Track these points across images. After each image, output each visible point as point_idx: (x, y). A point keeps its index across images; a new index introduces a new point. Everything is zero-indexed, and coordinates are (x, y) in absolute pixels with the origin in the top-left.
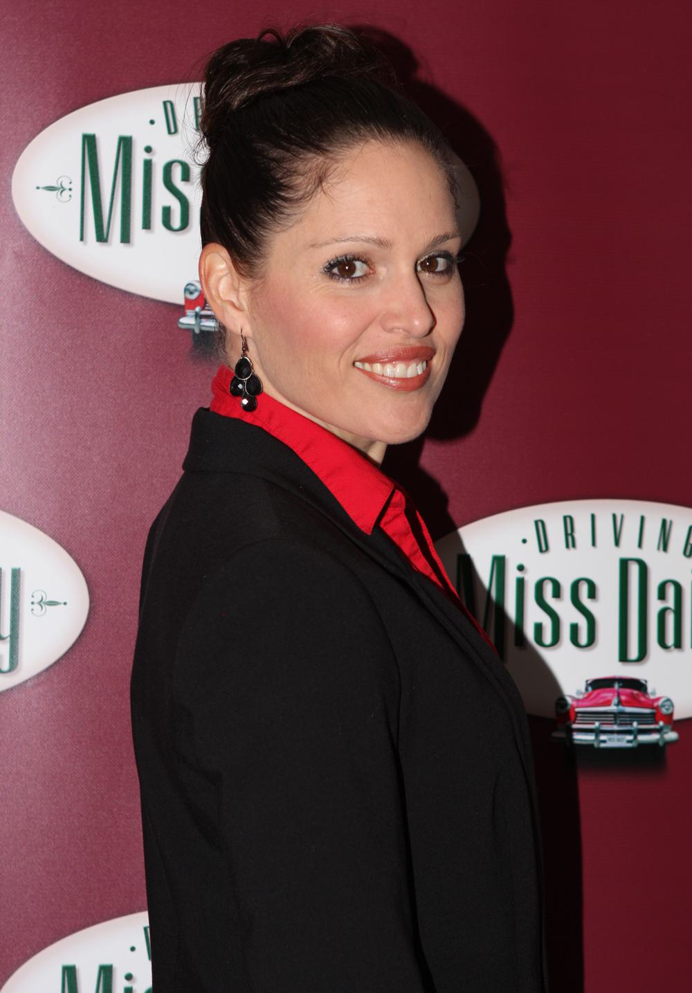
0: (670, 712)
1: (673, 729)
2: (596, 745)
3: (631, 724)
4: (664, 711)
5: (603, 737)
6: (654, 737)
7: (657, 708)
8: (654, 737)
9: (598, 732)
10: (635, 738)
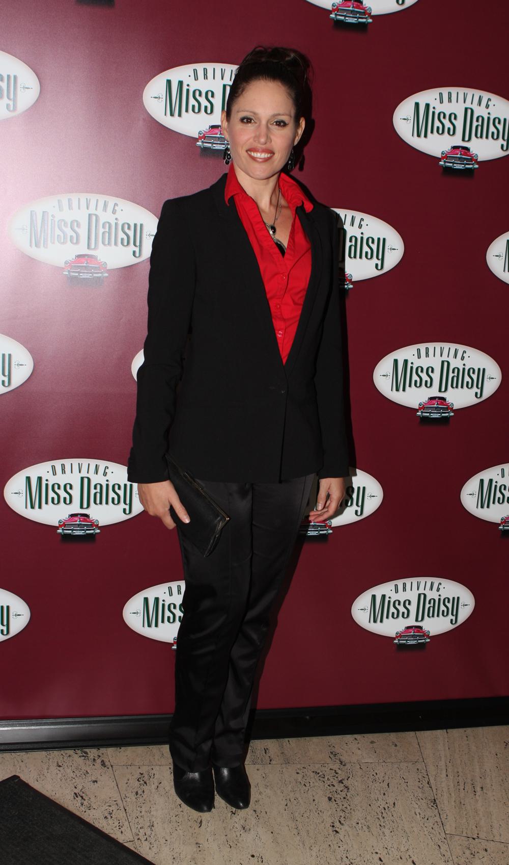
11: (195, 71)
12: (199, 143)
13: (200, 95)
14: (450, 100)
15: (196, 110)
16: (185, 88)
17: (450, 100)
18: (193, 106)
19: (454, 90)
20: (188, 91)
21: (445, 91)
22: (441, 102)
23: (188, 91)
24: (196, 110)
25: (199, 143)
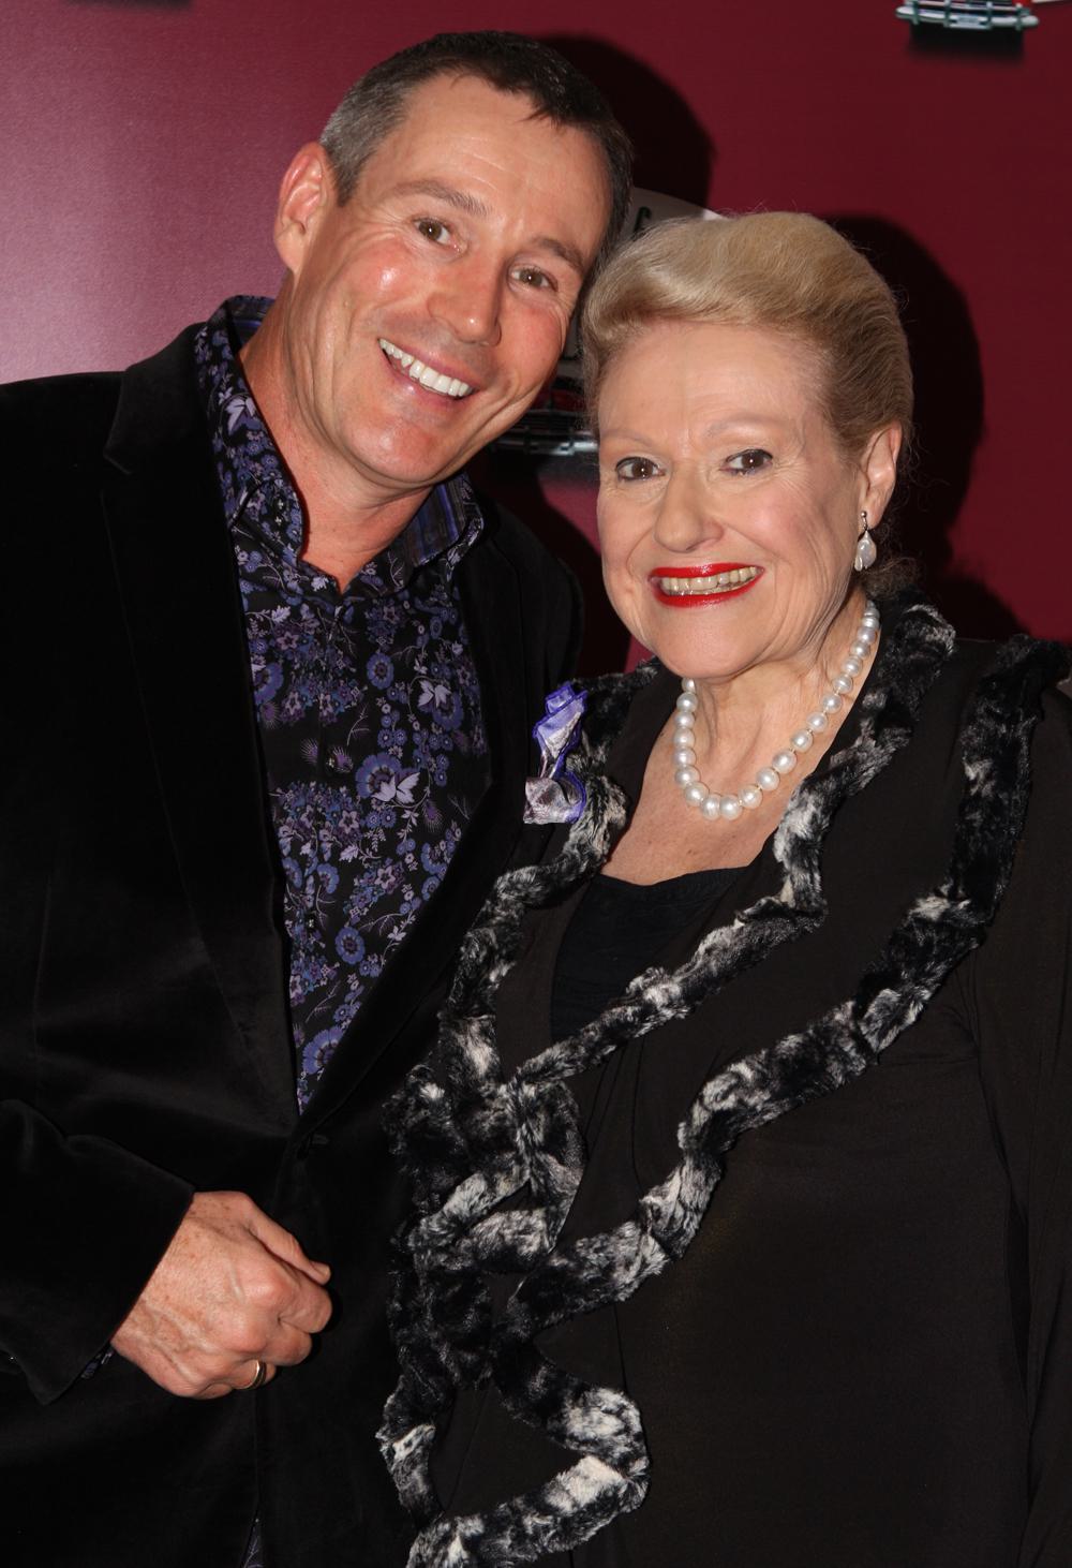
1: (1033, 13)
2: (946, 24)
3: (984, 4)
5: (953, 17)
6: (1011, 20)
8: (1010, 20)
9: (948, 10)
10: (989, 20)
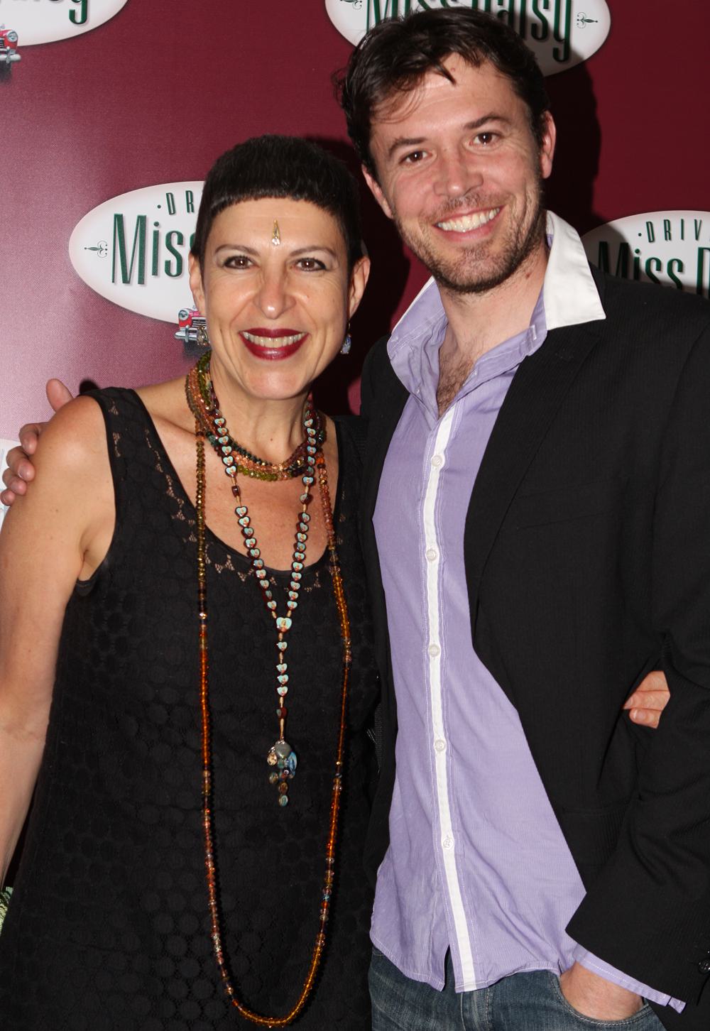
0: (15, 40)
1: (16, 53)
4: (10, 39)
7: (5, 37)
11: (170, 197)
12: (181, 334)
13: (181, 242)
14: (668, 235)
15: (174, 271)
16: (150, 229)
17: (668, 235)
18: (168, 264)
19: (675, 217)
20: (156, 234)
21: (657, 218)
22: (652, 239)
23: (156, 234)
24: (174, 271)
25: (181, 334)
